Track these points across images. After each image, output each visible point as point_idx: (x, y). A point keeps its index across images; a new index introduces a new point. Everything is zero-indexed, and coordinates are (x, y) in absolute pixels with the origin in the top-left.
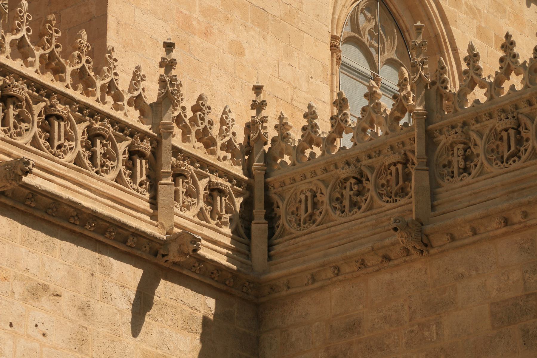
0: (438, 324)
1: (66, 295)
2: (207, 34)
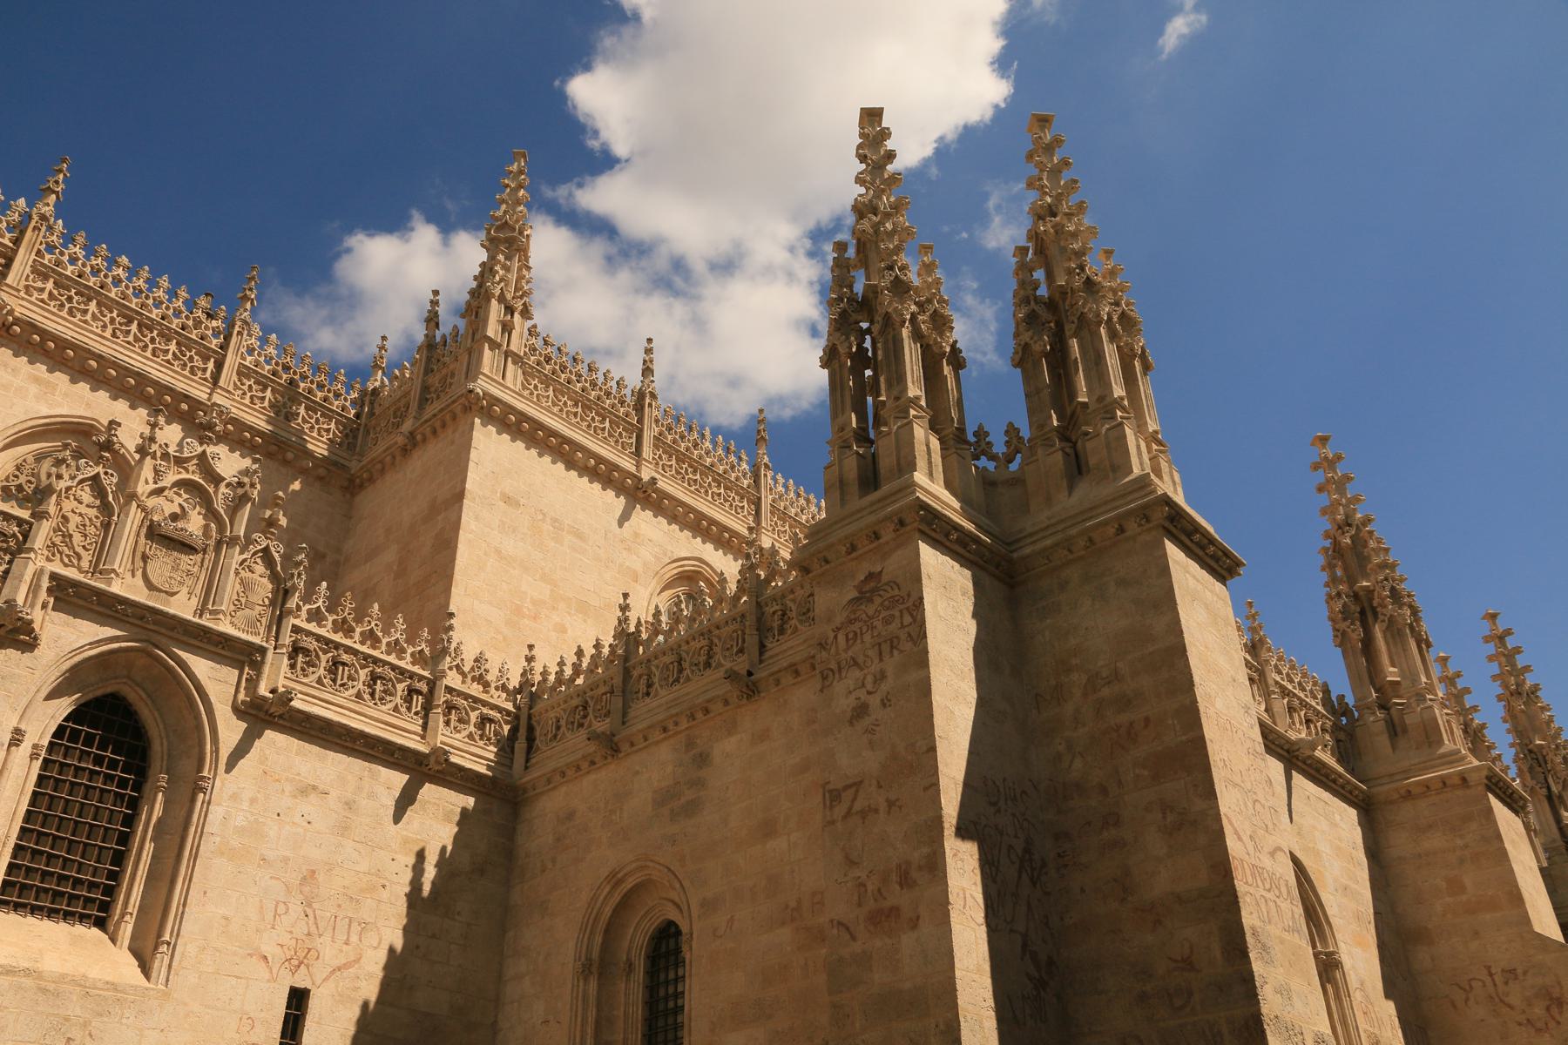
1: (334, 794)
2: (535, 618)
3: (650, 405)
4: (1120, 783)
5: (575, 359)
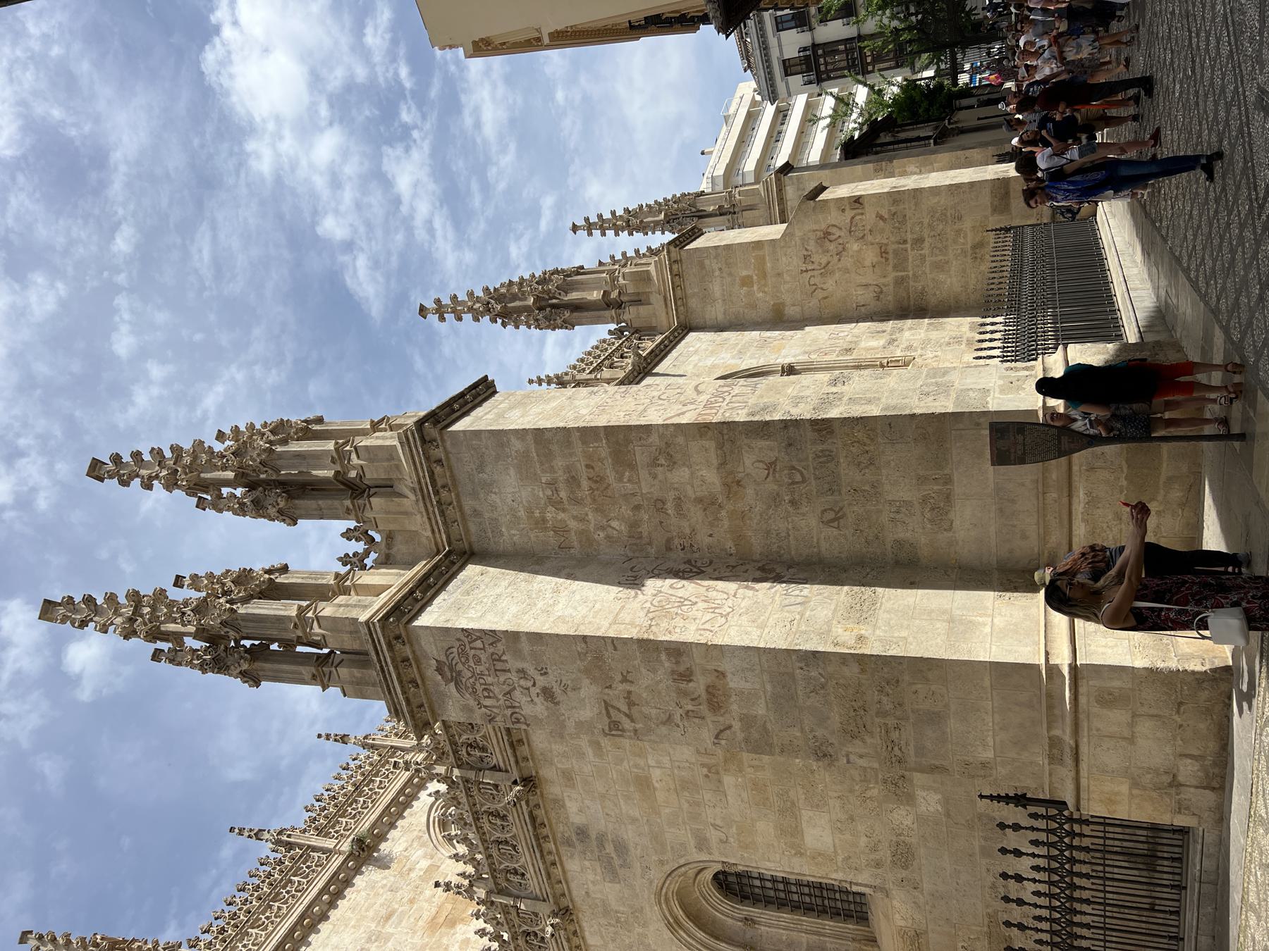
3: (289, 836)
5: (230, 904)
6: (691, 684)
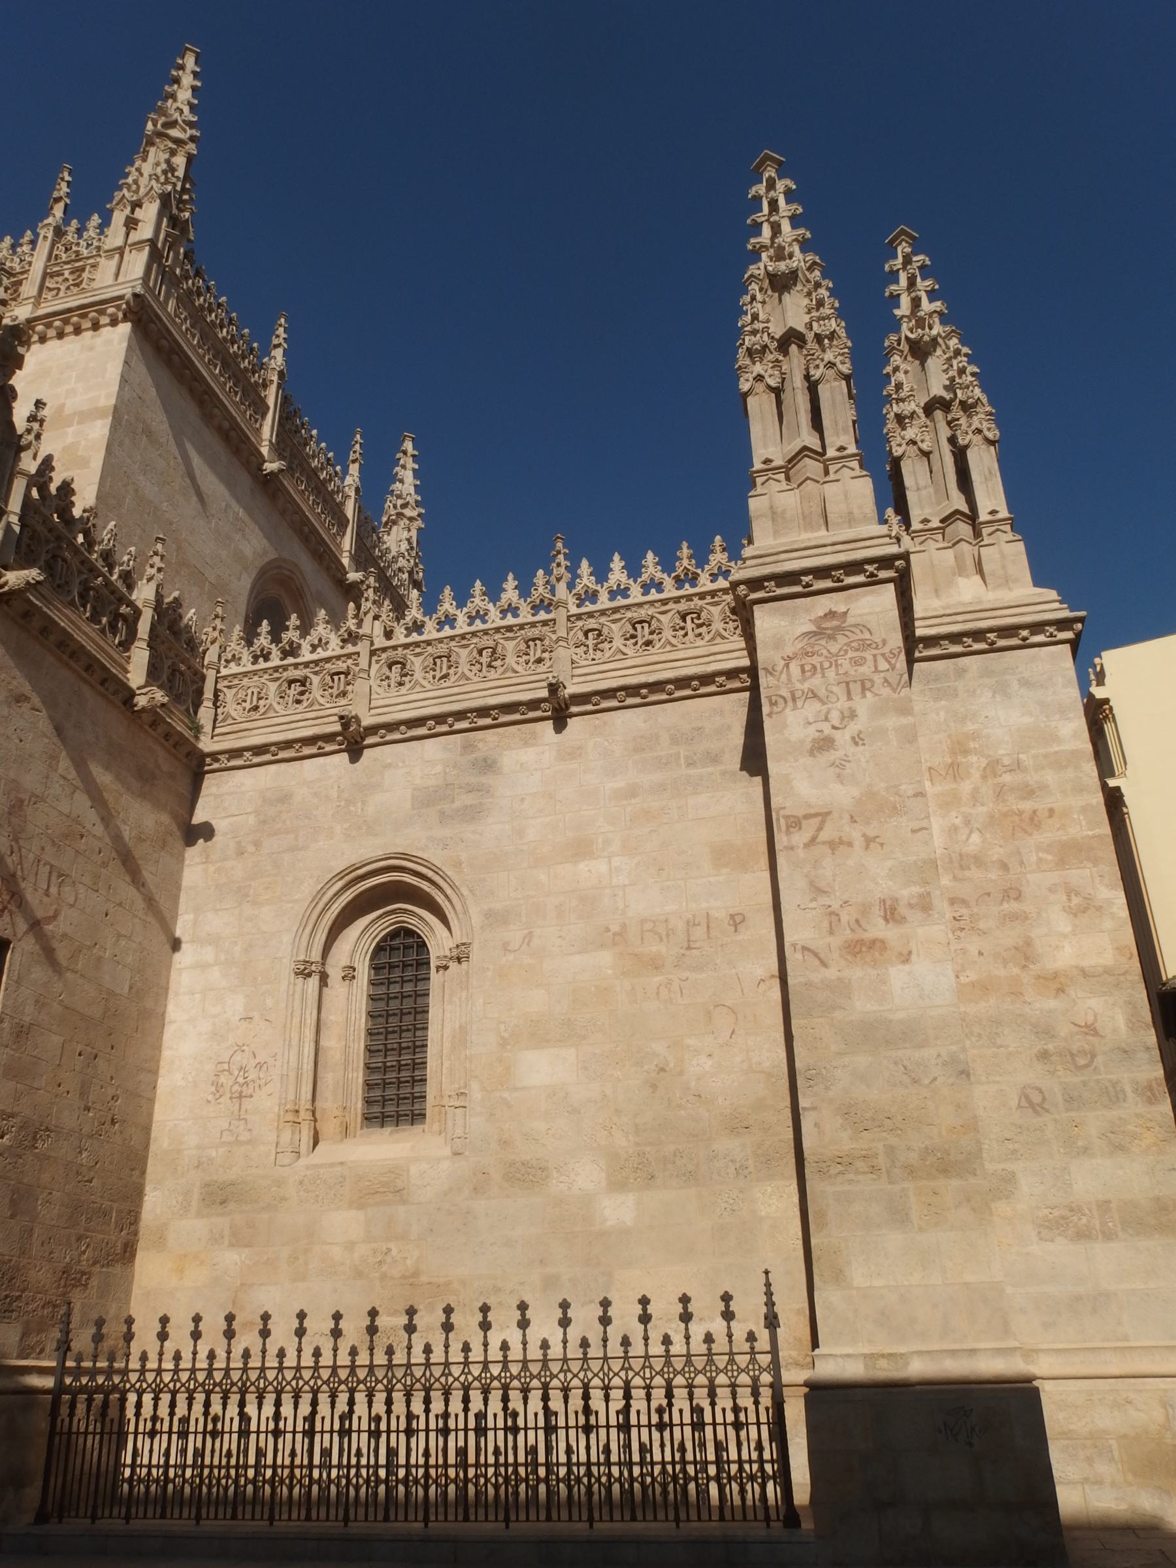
0: (364, 803)
4: (1022, 863)
6: (881, 921)
